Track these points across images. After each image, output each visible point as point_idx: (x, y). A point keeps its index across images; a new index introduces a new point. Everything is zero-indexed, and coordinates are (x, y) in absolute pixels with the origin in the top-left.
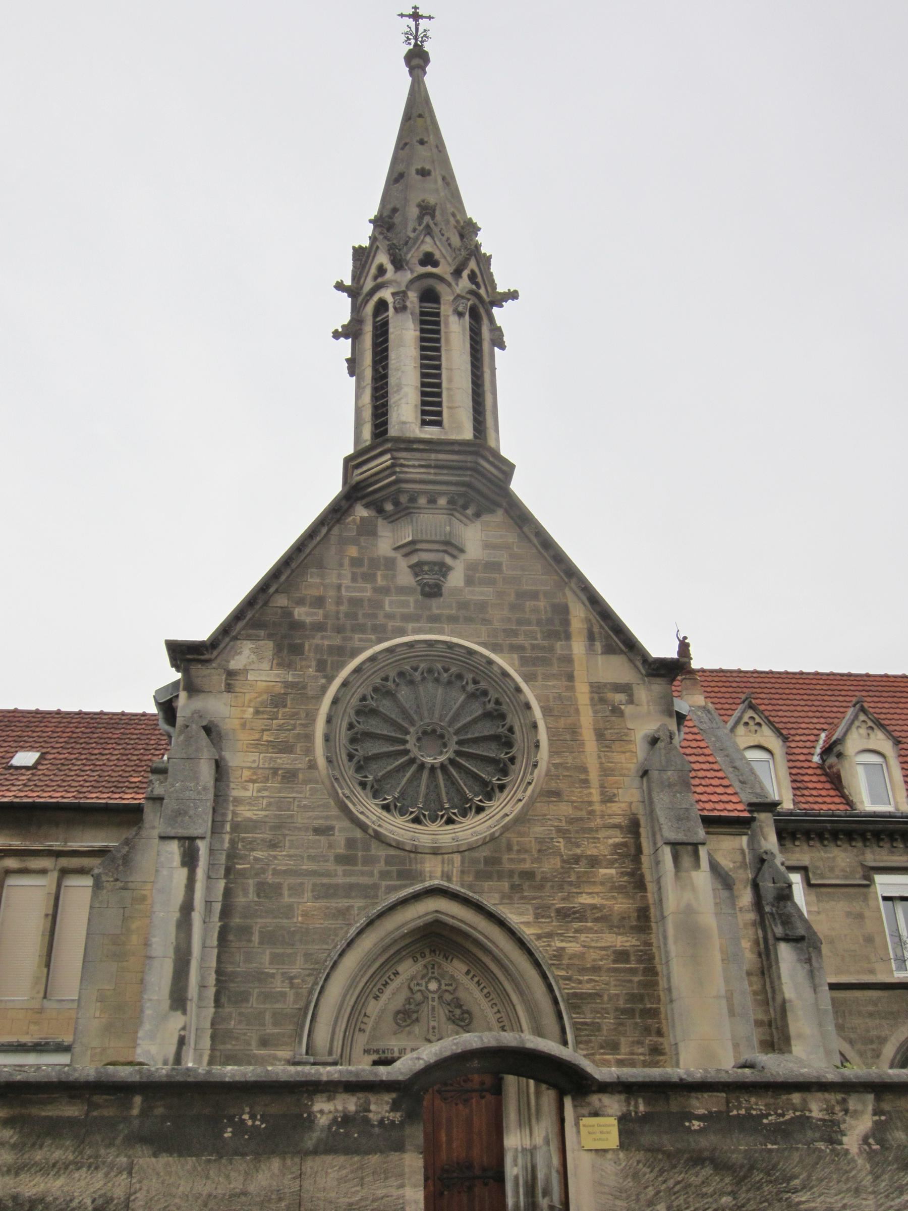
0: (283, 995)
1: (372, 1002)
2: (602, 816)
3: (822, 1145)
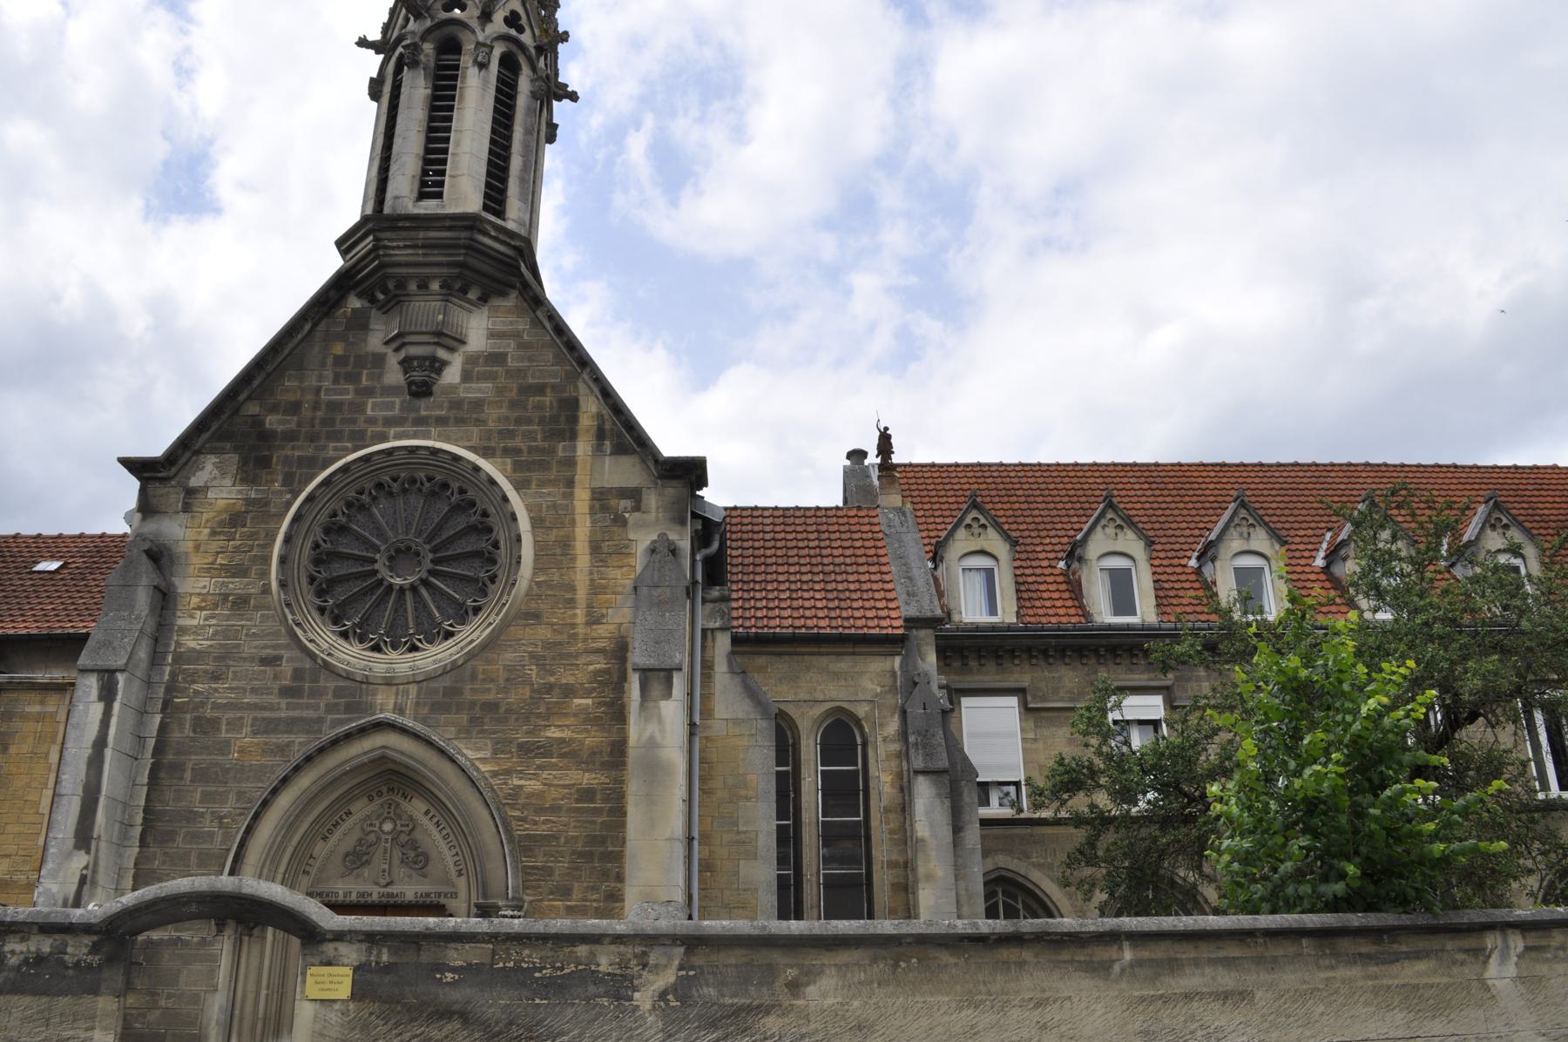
0: (211, 835)
1: (321, 844)
2: (585, 640)
3: (605, 1001)
